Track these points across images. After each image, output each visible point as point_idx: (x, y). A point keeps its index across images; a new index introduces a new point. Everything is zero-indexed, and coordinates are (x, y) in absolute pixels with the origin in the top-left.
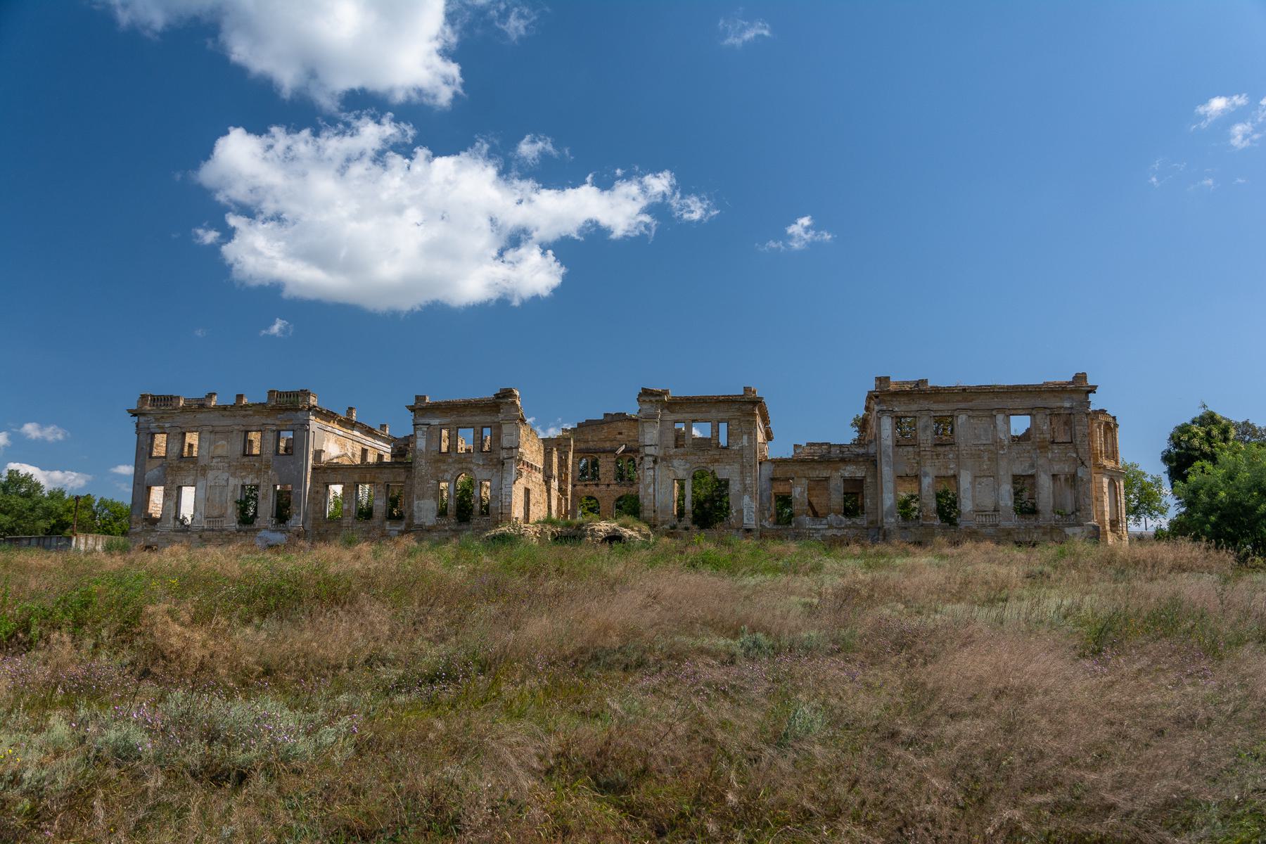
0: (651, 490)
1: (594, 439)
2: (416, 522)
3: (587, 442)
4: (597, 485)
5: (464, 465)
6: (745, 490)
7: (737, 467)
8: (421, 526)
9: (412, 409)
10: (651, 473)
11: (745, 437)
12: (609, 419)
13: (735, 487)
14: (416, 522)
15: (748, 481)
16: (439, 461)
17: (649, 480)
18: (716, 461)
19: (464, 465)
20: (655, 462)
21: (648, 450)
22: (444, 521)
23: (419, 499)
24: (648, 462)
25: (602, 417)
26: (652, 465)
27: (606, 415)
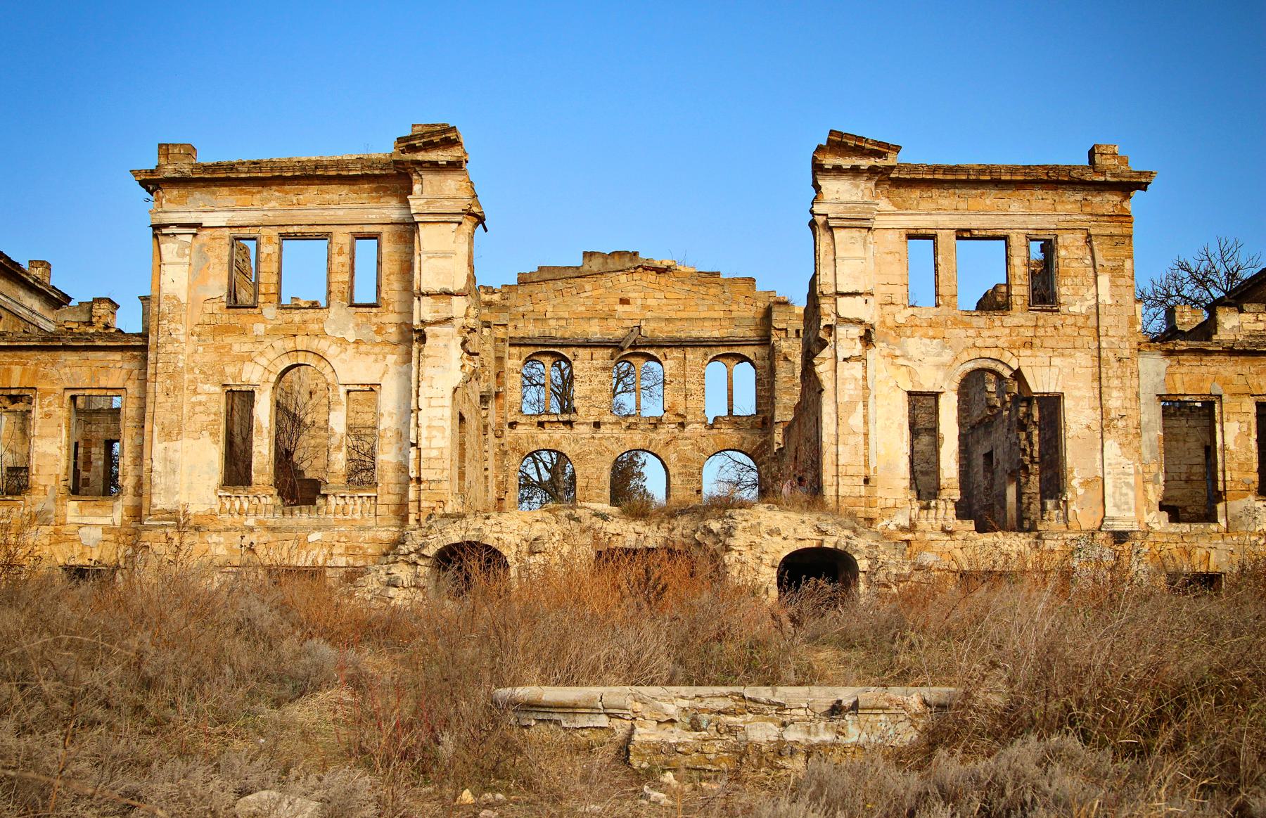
0: (856, 421)
1: (562, 314)
3: (543, 319)
4: (569, 423)
6: (1106, 424)
7: (1084, 361)
8: (172, 514)
12: (596, 265)
14: (160, 501)
15: (1115, 402)
16: (228, 329)
19: (301, 343)
20: (867, 339)
21: (848, 307)
22: (242, 501)
23: (167, 435)
24: (847, 341)
25: (578, 261)
26: (858, 349)
27: (588, 255)
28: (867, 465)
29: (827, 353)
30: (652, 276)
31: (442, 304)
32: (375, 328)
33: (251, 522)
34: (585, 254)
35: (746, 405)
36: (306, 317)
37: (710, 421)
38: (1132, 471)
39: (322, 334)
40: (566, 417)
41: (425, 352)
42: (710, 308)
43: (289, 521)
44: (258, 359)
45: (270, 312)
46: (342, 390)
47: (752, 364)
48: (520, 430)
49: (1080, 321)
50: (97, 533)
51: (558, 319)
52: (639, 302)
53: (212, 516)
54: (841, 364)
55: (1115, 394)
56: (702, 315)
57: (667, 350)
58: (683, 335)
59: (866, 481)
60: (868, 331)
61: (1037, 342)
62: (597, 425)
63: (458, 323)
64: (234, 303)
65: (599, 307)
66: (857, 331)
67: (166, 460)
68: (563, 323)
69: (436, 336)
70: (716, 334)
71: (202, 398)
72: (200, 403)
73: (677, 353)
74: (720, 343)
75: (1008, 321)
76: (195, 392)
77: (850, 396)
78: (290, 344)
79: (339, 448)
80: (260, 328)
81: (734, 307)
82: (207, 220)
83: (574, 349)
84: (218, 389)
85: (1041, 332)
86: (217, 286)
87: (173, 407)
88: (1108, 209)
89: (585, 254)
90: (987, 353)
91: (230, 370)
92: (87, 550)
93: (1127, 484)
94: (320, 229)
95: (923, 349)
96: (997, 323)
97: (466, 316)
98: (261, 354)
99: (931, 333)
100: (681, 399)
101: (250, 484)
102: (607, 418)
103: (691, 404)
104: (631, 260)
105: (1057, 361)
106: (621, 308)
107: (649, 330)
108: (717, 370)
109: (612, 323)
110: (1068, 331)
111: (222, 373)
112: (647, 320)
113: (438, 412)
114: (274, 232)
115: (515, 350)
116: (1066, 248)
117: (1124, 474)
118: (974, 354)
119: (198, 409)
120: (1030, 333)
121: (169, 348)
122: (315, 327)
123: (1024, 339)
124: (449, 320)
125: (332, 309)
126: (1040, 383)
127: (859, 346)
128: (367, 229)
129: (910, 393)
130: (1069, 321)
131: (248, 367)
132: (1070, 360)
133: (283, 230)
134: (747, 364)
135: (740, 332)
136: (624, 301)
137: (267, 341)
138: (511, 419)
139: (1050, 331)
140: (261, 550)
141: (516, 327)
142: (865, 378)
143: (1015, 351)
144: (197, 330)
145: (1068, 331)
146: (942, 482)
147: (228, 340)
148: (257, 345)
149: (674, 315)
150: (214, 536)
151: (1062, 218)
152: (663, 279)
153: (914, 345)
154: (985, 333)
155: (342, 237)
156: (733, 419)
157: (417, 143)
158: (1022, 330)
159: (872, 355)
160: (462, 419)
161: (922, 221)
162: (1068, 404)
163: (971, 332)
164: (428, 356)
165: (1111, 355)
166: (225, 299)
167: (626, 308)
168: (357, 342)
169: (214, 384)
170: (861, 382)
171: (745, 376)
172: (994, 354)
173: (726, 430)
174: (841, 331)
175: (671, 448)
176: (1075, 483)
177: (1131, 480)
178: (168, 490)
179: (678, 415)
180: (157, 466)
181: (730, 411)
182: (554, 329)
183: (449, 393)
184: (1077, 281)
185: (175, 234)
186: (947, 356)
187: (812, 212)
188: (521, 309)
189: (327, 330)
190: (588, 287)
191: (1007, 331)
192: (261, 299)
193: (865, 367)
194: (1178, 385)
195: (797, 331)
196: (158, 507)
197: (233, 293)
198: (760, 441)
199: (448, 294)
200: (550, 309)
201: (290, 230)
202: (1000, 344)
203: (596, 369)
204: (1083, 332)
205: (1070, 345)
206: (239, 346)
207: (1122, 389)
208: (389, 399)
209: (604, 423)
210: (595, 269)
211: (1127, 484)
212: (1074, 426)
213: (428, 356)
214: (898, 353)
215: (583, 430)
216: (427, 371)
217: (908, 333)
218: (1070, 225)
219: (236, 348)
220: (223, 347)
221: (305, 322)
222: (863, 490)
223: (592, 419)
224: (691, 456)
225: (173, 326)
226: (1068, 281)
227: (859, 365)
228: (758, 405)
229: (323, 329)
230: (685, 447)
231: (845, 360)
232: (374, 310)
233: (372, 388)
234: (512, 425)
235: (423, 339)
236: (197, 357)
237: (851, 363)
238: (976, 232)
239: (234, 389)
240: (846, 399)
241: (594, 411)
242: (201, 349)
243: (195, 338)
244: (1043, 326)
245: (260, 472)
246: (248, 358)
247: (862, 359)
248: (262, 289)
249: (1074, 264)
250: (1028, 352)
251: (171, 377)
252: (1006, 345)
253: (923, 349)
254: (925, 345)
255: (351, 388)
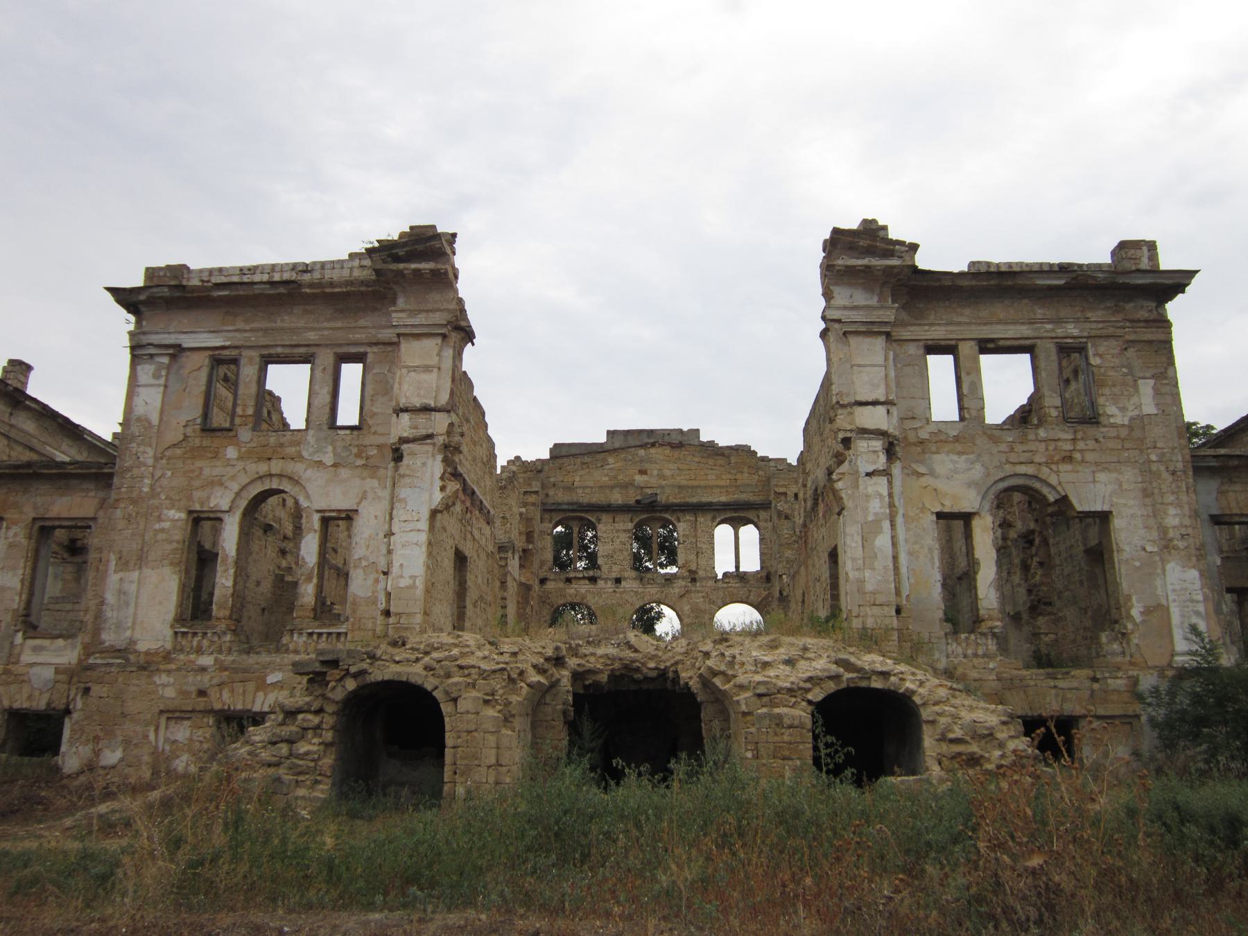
0: (883, 541)
1: (588, 485)
2: (108, 638)
3: (570, 488)
4: (593, 580)
5: (276, 466)
9: (124, 297)
10: (881, 484)
11: (1146, 387)
13: (1130, 536)
14: (108, 638)
17: (876, 507)
18: (1068, 459)
19: (276, 466)
20: (890, 451)
23: (124, 565)
25: (602, 438)
28: (898, 592)
29: (845, 467)
30: (668, 451)
31: (421, 419)
32: (355, 450)
33: (207, 660)
34: (608, 432)
35: (751, 563)
36: (283, 440)
37: (720, 576)
38: (1200, 598)
39: (298, 457)
40: (591, 573)
41: (401, 471)
42: (719, 477)
43: (251, 660)
44: (228, 483)
45: (245, 434)
46: (316, 517)
47: (756, 526)
48: (550, 585)
49: (1124, 433)
50: (49, 673)
51: (584, 488)
52: (655, 472)
53: (167, 657)
54: (863, 481)
55: (1172, 511)
56: (711, 483)
57: (680, 514)
58: (694, 500)
59: (898, 611)
60: (891, 444)
61: (1078, 456)
62: (618, 581)
63: (440, 440)
64: (207, 429)
65: (620, 477)
66: (878, 444)
67: (121, 592)
68: (587, 491)
69: (413, 454)
70: (723, 499)
71: (167, 525)
72: (163, 530)
73: (689, 517)
74: (726, 507)
75: (1042, 433)
76: (159, 519)
77: (876, 514)
78: (263, 468)
79: (309, 579)
80: (231, 452)
81: (739, 476)
82: (188, 341)
83: (598, 514)
84: (183, 515)
85: (1081, 445)
86: (192, 410)
87: (133, 535)
88: (1143, 314)
89: (608, 432)
90: (1022, 469)
91: (197, 494)
92: (37, 693)
93: (1197, 613)
94: (302, 350)
95: (951, 466)
96: (1031, 436)
97: (449, 433)
98: (233, 478)
99: (959, 447)
100: (693, 557)
101: (210, 618)
102: (626, 574)
103: (702, 562)
104: (649, 437)
105: (1101, 477)
106: (639, 479)
107: (662, 499)
108: (723, 533)
109: (631, 491)
110: (1111, 444)
111: (190, 498)
112: (662, 487)
113: (414, 537)
114: (255, 354)
115: (547, 516)
116: (1101, 356)
117: (1192, 601)
118: (1009, 469)
119: (161, 536)
120: (1068, 446)
121: (135, 472)
122: (291, 450)
123: (1064, 454)
124: (430, 436)
125: (311, 432)
126: (1084, 501)
127: (883, 458)
128: (353, 350)
129: (940, 516)
130: (1113, 433)
131: (218, 491)
132: (1114, 475)
133: (266, 352)
134: (751, 527)
135: (744, 497)
136: (643, 472)
137: (240, 465)
138: (542, 575)
139: (1091, 444)
140: (213, 694)
141: (547, 495)
142: (890, 495)
143: (1053, 467)
144: (167, 453)
145: (1111, 444)
146: (982, 612)
147: (199, 463)
148: (229, 468)
149: (684, 482)
150: (164, 675)
151: (1094, 326)
152: (676, 453)
153: (944, 462)
154: (1019, 448)
155: (326, 358)
156: (739, 576)
157: (401, 253)
158: (1060, 444)
159: (896, 469)
160: (461, 560)
161: (938, 333)
162: (1117, 523)
163: (1003, 447)
164: (403, 476)
165: (1162, 468)
166: (199, 421)
167: (645, 478)
168: (335, 465)
169: (179, 510)
170: (887, 499)
171: (750, 534)
172: (1030, 470)
173: (734, 584)
174: (862, 445)
175: (685, 599)
176: (1135, 612)
177: (1201, 608)
178: (119, 626)
179: (690, 571)
180: (110, 597)
181: (737, 567)
182: (584, 497)
183: (426, 515)
184: (1116, 390)
185: (152, 356)
186: (977, 472)
187: (824, 318)
188: (552, 480)
189: (305, 454)
190: (611, 460)
191: (1043, 445)
192: (238, 421)
193: (890, 483)
194: (1233, 504)
195: (796, 496)
196: (107, 644)
197: (206, 415)
198: (765, 593)
199: (426, 409)
200: (577, 479)
201: (272, 351)
202: (1038, 459)
203: (618, 531)
204: (1127, 445)
205: (1115, 459)
206: (210, 470)
207: (1179, 505)
208: (367, 526)
209: (625, 579)
210: (617, 445)
211: (1197, 613)
212: (1127, 548)
213: (403, 476)
214: (922, 469)
215: (606, 586)
216: (403, 493)
217: (934, 449)
218: (1104, 332)
219: (207, 472)
220: (193, 471)
221: (282, 445)
222: (895, 623)
223: (614, 575)
224: (703, 607)
225: (142, 449)
226: (1107, 391)
227: (884, 480)
228: (762, 561)
229: (299, 453)
230: (698, 599)
231: (868, 474)
232: (355, 433)
233: (349, 516)
234: (543, 581)
235: (398, 457)
236: (164, 482)
237: (875, 479)
238: (1001, 343)
239: (203, 515)
240: (870, 518)
241: (615, 568)
242: (169, 473)
243: (164, 461)
244: (1083, 439)
245: (221, 607)
246: (220, 483)
247: (886, 473)
248: (239, 411)
249: (1111, 373)
250: (1068, 467)
251: (134, 502)
252: (1044, 460)
253: (951, 466)
254: (952, 461)
255: (327, 514)
